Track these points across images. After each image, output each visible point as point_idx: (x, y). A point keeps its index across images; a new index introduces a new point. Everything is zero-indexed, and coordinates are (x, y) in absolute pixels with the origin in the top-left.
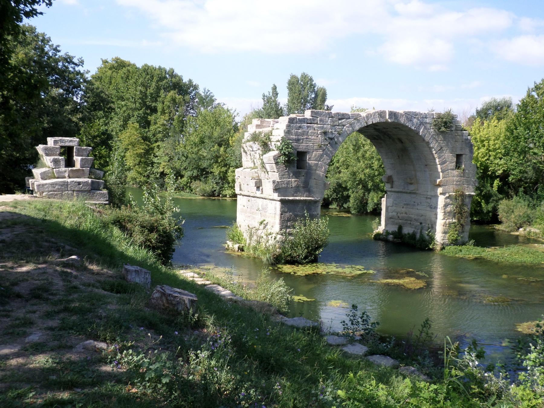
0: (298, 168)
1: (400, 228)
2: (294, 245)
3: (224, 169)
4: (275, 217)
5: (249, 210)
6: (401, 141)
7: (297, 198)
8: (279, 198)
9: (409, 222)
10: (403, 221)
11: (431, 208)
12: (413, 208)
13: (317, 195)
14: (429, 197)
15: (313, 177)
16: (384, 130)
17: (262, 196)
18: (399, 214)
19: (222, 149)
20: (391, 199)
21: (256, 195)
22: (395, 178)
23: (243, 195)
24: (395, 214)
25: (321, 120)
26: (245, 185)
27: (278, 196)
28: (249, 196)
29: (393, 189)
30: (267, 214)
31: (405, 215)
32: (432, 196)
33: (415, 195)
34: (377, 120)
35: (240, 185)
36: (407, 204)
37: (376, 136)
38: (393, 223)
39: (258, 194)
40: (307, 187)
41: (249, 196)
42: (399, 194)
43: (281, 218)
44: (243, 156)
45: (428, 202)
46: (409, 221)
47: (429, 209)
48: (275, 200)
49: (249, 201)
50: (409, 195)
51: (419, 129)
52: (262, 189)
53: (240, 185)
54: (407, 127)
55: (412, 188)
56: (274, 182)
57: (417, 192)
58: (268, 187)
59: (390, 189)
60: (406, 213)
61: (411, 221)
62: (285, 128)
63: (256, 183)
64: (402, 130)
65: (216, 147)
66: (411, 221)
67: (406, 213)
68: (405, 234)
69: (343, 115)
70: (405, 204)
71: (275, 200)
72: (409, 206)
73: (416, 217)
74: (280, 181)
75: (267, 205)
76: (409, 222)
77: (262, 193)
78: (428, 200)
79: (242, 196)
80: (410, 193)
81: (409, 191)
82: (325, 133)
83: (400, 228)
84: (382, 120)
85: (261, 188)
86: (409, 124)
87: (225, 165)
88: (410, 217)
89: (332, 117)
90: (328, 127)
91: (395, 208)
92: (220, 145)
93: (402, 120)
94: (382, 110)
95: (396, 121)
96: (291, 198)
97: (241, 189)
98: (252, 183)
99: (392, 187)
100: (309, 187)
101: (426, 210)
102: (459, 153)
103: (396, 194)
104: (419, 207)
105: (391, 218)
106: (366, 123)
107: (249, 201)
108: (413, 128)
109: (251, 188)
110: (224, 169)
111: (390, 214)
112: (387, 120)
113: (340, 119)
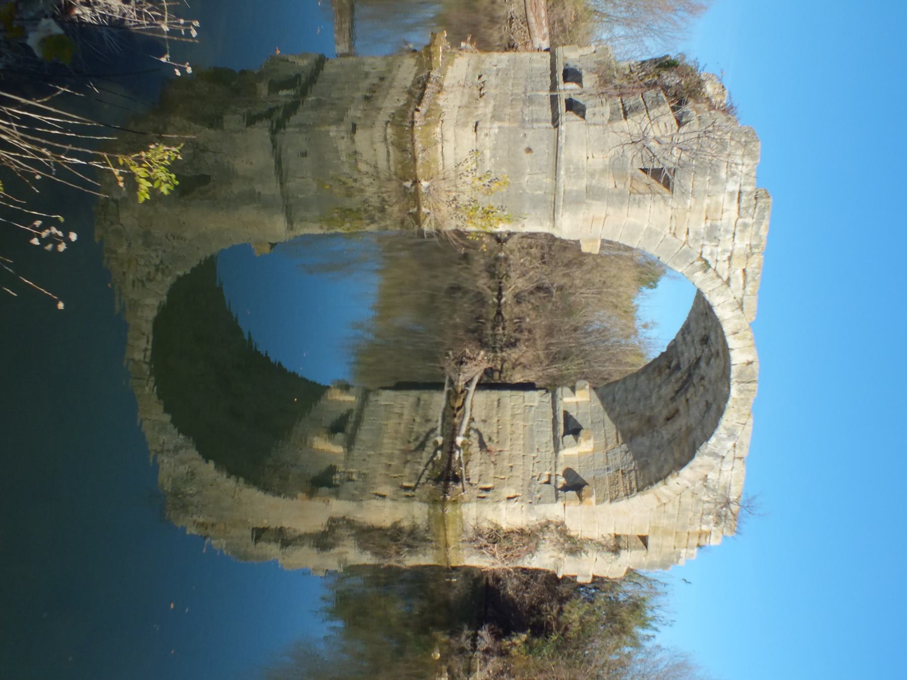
15: (611, 211)
16: (695, 380)
25: (745, 225)
40: (588, 197)
54: (716, 425)
67: (513, 433)
70: (531, 430)
75: (541, 104)
86: (721, 431)
102: (651, 541)
108: (713, 440)
113: (744, 270)
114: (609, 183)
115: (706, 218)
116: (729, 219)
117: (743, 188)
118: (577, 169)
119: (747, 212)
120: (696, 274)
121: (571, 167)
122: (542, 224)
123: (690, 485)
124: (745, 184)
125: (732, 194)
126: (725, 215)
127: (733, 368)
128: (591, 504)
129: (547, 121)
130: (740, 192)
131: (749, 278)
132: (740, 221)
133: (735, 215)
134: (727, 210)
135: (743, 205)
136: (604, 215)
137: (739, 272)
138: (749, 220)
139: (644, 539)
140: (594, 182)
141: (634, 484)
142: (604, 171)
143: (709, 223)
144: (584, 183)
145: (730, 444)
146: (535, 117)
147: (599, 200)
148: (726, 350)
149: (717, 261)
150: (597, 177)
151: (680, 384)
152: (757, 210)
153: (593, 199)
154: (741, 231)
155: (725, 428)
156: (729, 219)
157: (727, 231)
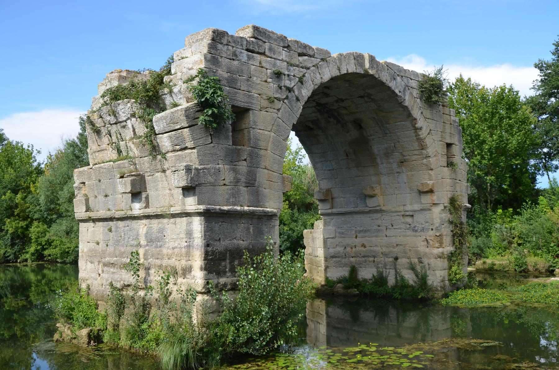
0: (234, 143)
1: (354, 271)
2: (237, 315)
3: (23, 224)
4: (188, 255)
5: (111, 249)
6: (358, 124)
7: (239, 208)
8: (202, 208)
9: (372, 259)
10: (358, 259)
11: (416, 231)
12: (376, 236)
13: (272, 203)
14: (407, 213)
15: (263, 164)
17: (149, 211)
18: (348, 249)
19: (19, 196)
20: (330, 227)
21: (129, 213)
22: (336, 193)
23: (95, 221)
24: (341, 249)
25: (270, 49)
26: (101, 198)
27: (199, 204)
28: (111, 219)
29: (334, 210)
30: (165, 251)
31: (363, 249)
32: (415, 211)
33: (379, 215)
34: (352, 68)
35: (87, 200)
36: (366, 231)
37: (313, 122)
38: (340, 265)
39: (137, 208)
40: (253, 185)
41: (111, 219)
42: (347, 216)
43: (206, 254)
44: (90, 142)
45: (406, 223)
46: (369, 257)
47: (409, 232)
48: (188, 215)
49: (110, 230)
50: (368, 215)
51: (405, 95)
52: (147, 198)
53: (87, 200)
54: (389, 88)
55: (371, 203)
56: (188, 169)
57: (383, 208)
58: (166, 189)
59: (330, 211)
60: (364, 246)
61: (374, 257)
62: (205, 50)
63: (133, 183)
64: (373, 100)
65: (9, 194)
66: (374, 257)
67: (364, 246)
68: (365, 281)
69: (305, 46)
70: (360, 232)
71: (188, 215)
72: (367, 234)
73: (384, 250)
74: (200, 167)
75: (161, 230)
76: (372, 259)
77: (147, 206)
78: (409, 220)
79: (91, 224)
80: (369, 212)
81: (367, 209)
82: (278, 75)
83: (354, 271)
84: (360, 71)
85: (144, 195)
86: (392, 85)
87: (25, 219)
88: (374, 251)
89: (288, 47)
90: (282, 67)
91: (340, 240)
92: (15, 191)
93: (385, 77)
94: (359, 52)
95: (377, 76)
96: (226, 208)
97: (88, 209)
98: (124, 186)
99: (332, 208)
100: (256, 184)
101: (404, 236)
102: (449, 142)
103: (339, 217)
104: (388, 233)
105: (332, 257)
106: (339, 70)
107: (110, 230)
108: (397, 91)
109: (119, 199)
110: (23, 224)
111: (332, 251)
112: (366, 71)
113: (300, 55)
114: (243, 167)
115: (266, 81)
116: (266, 62)
117: (245, 47)
118: (234, 195)
119: (261, 46)
120: (304, 94)
121: (231, 200)
122: (274, 226)
123: (420, 111)
124: (242, 45)
125: (249, 58)
126: (264, 64)
127: (358, 71)
128: (433, 184)
129: (189, 224)
130: (248, 50)
131: (304, 51)
132: (267, 53)
133: (263, 58)
134: (260, 63)
135: (257, 50)
136: (266, 171)
137: (301, 58)
138: (267, 45)
139: (449, 145)
140: (243, 180)
141: (416, 152)
142: (235, 171)
143: (269, 80)
144: (243, 189)
145: (399, 79)
146: (183, 235)
147: (256, 176)
148: (347, 74)
149: (294, 76)
150: (240, 177)
151: (332, 120)
152: (260, 37)
153: (255, 180)
154: (274, 54)
155: (390, 82)
156: (266, 62)
157: (274, 65)
